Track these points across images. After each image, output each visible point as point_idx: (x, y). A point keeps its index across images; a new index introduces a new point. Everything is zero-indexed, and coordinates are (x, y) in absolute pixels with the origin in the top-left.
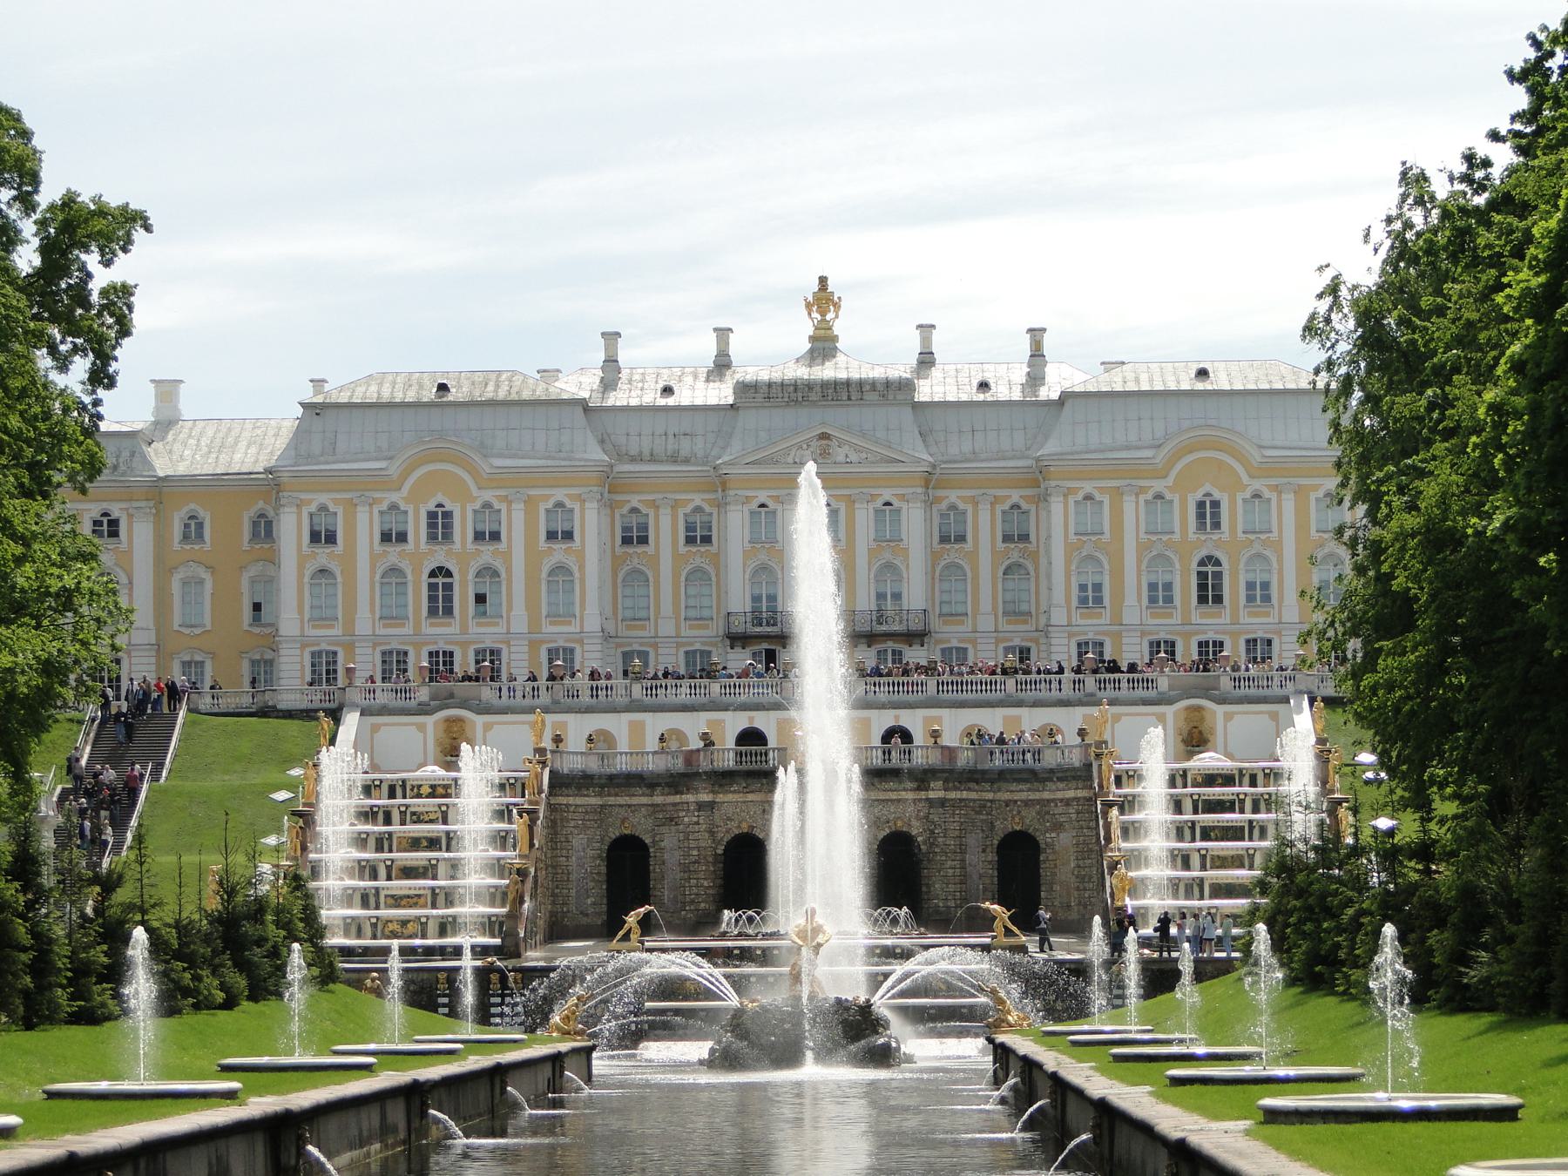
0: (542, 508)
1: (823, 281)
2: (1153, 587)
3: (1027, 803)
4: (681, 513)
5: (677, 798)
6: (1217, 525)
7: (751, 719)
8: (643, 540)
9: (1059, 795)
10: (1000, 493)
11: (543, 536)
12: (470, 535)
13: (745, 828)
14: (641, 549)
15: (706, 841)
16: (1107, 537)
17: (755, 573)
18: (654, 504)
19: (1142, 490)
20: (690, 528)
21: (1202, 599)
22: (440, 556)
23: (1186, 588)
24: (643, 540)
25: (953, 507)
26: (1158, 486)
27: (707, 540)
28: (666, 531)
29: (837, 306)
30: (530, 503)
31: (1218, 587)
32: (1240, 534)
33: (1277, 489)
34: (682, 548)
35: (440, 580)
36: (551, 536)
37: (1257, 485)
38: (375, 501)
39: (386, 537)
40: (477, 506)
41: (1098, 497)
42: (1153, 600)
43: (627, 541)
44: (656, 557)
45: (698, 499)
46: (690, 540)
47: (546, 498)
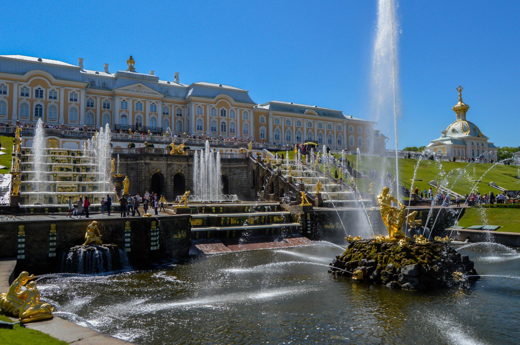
0: (69, 92)
1: (131, 57)
2: (212, 128)
3: (226, 168)
4: (102, 100)
5: (138, 162)
6: (225, 115)
7: (140, 145)
8: (92, 106)
9: (235, 166)
10: (177, 105)
11: (69, 99)
12: (48, 97)
13: (158, 171)
14: (92, 108)
15: (147, 175)
16: (203, 115)
17: (122, 116)
18: (95, 97)
19: (211, 106)
20: (104, 104)
21: (222, 130)
22: (39, 101)
23: (218, 128)
24: (92, 106)
25: (166, 107)
26: (214, 106)
27: (108, 108)
28: (98, 104)
29: (134, 63)
30: (66, 91)
31: (225, 128)
32: (230, 118)
33: (236, 109)
34: (103, 109)
35: (39, 107)
36: (71, 100)
37: (233, 108)
38: (20, 85)
39: (22, 94)
40: (51, 89)
41: (201, 106)
42: (212, 130)
43: (88, 106)
44: (95, 111)
45: (107, 98)
46: (104, 107)
47: (70, 90)
